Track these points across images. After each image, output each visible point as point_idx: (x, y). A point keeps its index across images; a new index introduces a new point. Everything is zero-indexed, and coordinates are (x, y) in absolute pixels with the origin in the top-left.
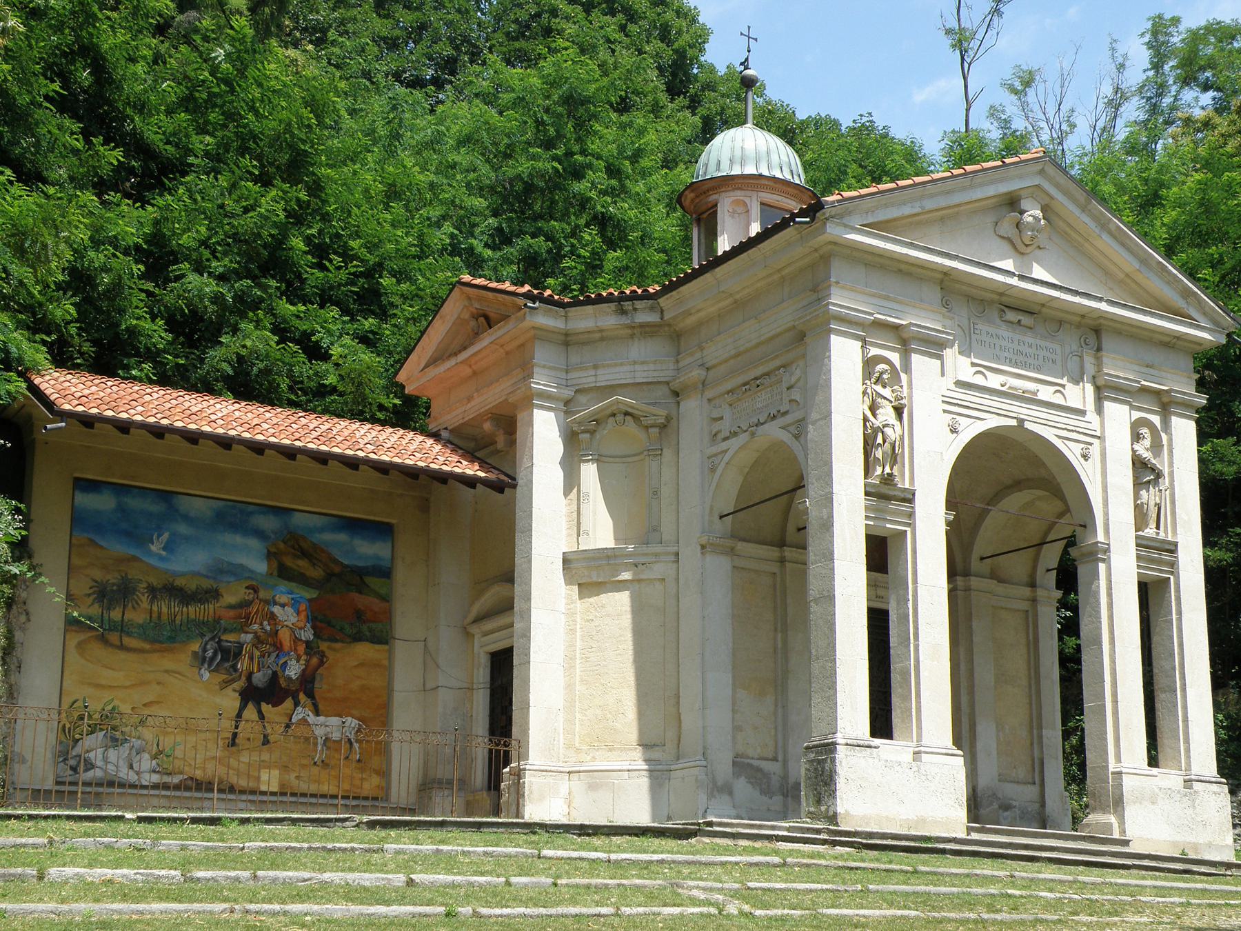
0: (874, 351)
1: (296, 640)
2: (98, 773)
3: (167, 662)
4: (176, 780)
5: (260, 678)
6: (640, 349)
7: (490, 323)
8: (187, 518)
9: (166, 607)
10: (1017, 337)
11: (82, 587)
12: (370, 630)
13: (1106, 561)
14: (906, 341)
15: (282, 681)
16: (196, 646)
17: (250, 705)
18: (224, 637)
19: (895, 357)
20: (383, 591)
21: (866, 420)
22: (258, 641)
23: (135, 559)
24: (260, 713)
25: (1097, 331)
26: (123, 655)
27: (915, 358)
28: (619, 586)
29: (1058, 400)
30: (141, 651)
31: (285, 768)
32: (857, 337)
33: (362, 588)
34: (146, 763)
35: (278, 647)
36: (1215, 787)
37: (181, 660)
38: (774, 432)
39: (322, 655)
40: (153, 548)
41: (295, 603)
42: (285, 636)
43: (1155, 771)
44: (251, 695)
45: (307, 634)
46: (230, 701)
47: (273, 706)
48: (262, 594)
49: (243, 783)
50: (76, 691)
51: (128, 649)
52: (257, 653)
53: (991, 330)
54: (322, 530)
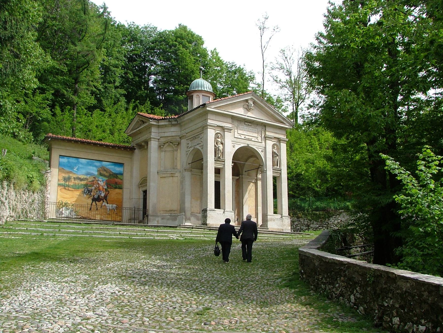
0: (217, 132)
1: (103, 188)
4: (80, 217)
5: (96, 196)
6: (173, 129)
7: (144, 122)
8: (81, 164)
9: (77, 182)
10: (248, 128)
11: (61, 178)
12: (119, 186)
13: (266, 173)
17: (94, 202)
18: (89, 188)
19: (222, 133)
20: (121, 178)
22: (96, 189)
23: (71, 172)
24: (96, 203)
25: (265, 126)
26: (69, 192)
27: (226, 132)
30: (72, 191)
31: (101, 215)
32: (214, 129)
33: (117, 177)
35: (100, 190)
36: (287, 218)
39: (109, 191)
40: (75, 170)
41: (103, 181)
42: (101, 187)
43: (275, 215)
44: (94, 200)
45: (106, 187)
46: (90, 201)
47: (99, 202)
48: (96, 179)
49: (92, 218)
50: (60, 199)
51: (70, 190)
52: (95, 191)
53: (242, 127)
54: (108, 165)
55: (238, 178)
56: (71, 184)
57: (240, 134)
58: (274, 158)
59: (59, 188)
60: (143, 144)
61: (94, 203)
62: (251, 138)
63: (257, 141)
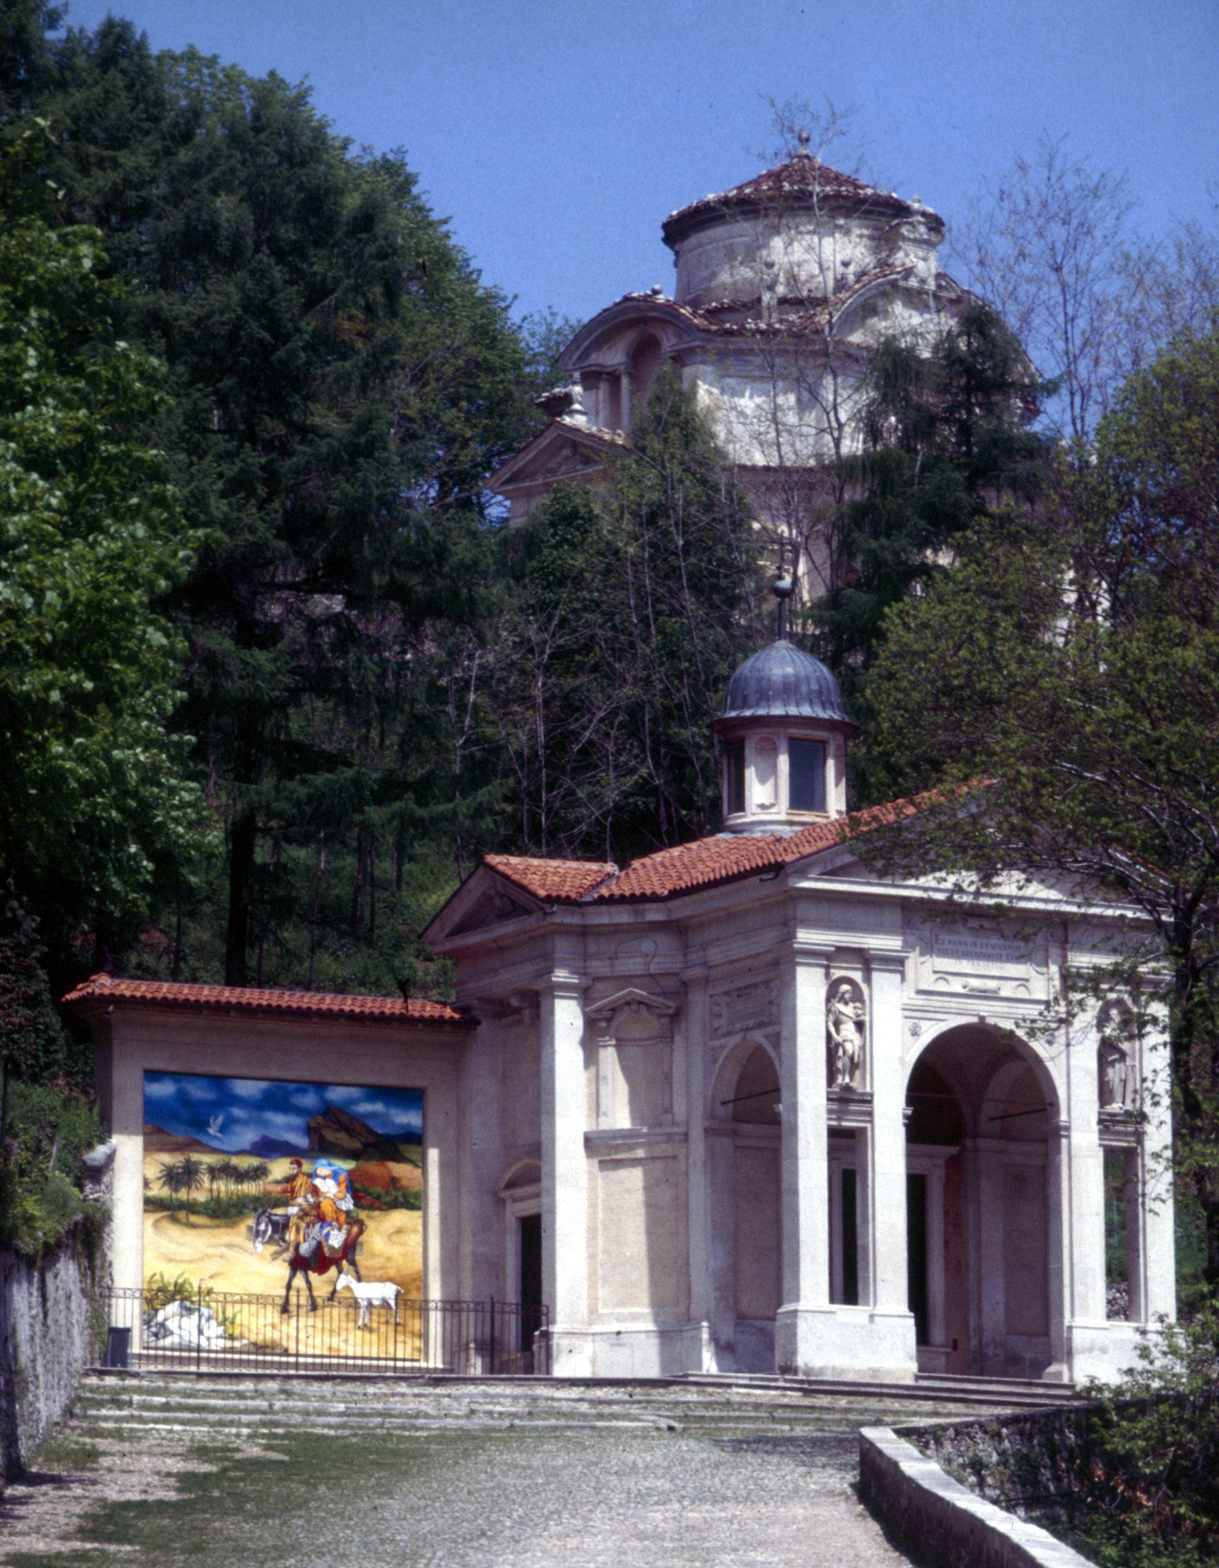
0: (837, 974)
1: (339, 1210)
2: (176, 1339)
3: (225, 1236)
5: (305, 1249)
10: (979, 941)
11: (153, 1172)
13: (1068, 1137)
14: (866, 960)
15: (326, 1250)
16: (251, 1222)
19: (857, 976)
21: (829, 1037)
28: (635, 1162)
29: (1022, 994)
34: (213, 1330)
35: (321, 1218)
37: (238, 1234)
38: (758, 1037)
40: (211, 1131)
41: (335, 1176)
42: (326, 1207)
44: (299, 1264)
45: (348, 1204)
46: (282, 1270)
53: (955, 938)
55: (954, 1150)
56: (200, 1196)
57: (943, 975)
58: (1110, 1071)
59: (152, 1218)
60: (515, 1002)
61: (299, 1281)
62: (992, 984)
63: (1026, 996)
